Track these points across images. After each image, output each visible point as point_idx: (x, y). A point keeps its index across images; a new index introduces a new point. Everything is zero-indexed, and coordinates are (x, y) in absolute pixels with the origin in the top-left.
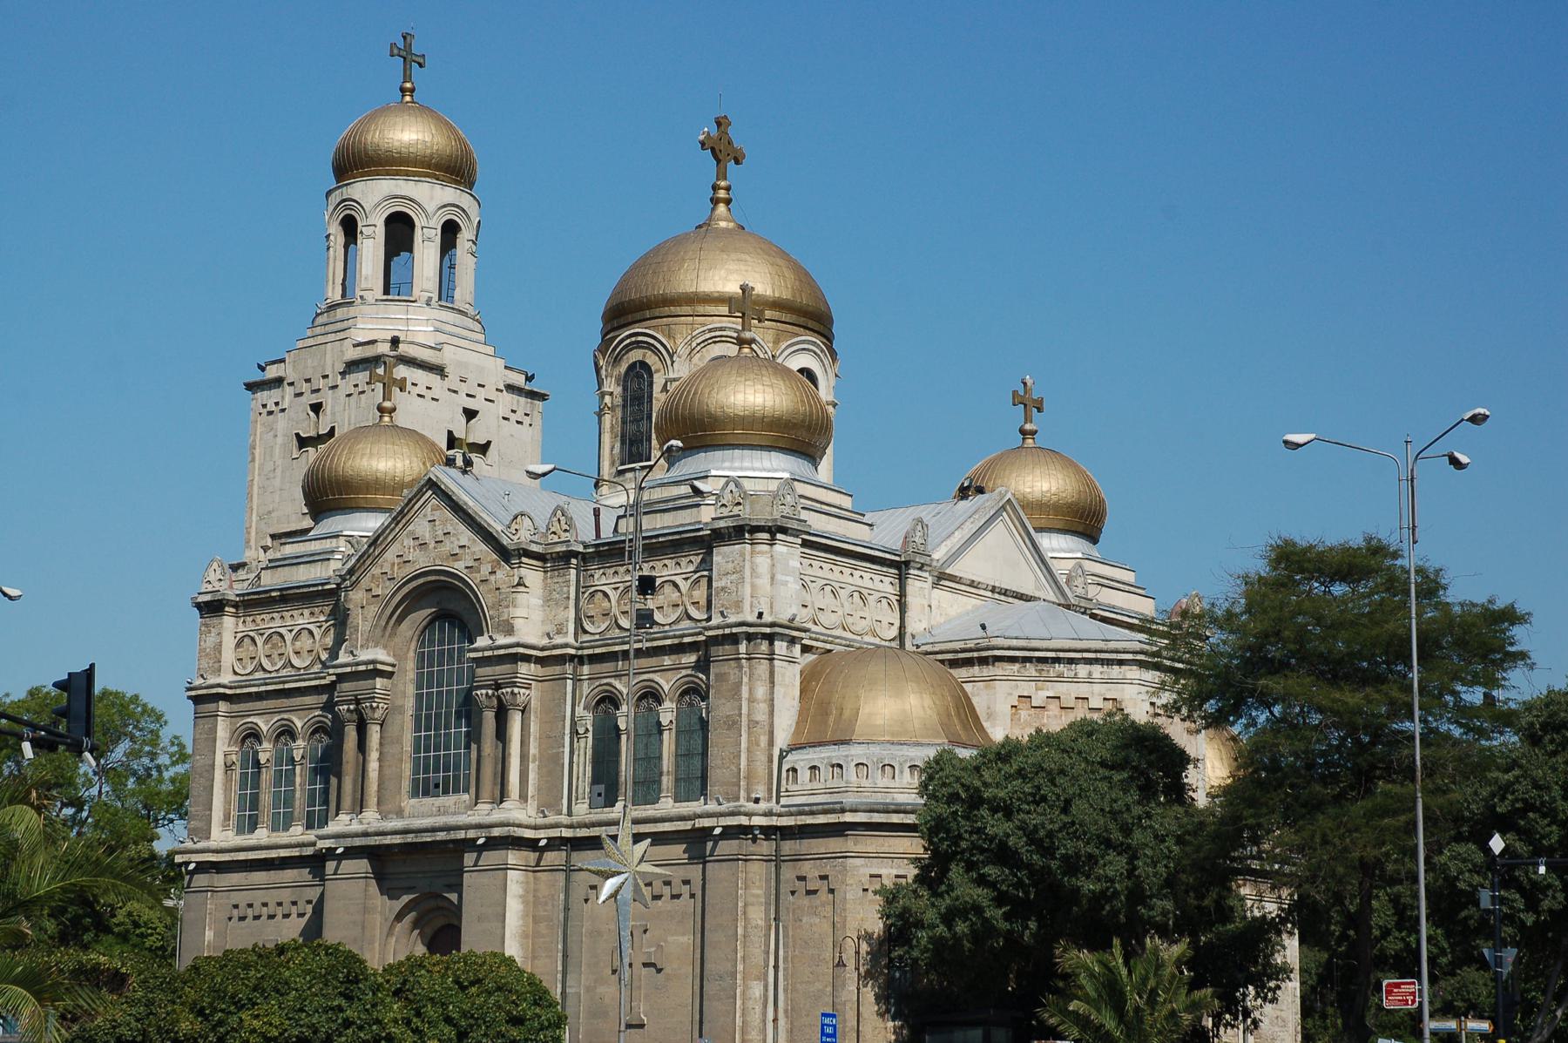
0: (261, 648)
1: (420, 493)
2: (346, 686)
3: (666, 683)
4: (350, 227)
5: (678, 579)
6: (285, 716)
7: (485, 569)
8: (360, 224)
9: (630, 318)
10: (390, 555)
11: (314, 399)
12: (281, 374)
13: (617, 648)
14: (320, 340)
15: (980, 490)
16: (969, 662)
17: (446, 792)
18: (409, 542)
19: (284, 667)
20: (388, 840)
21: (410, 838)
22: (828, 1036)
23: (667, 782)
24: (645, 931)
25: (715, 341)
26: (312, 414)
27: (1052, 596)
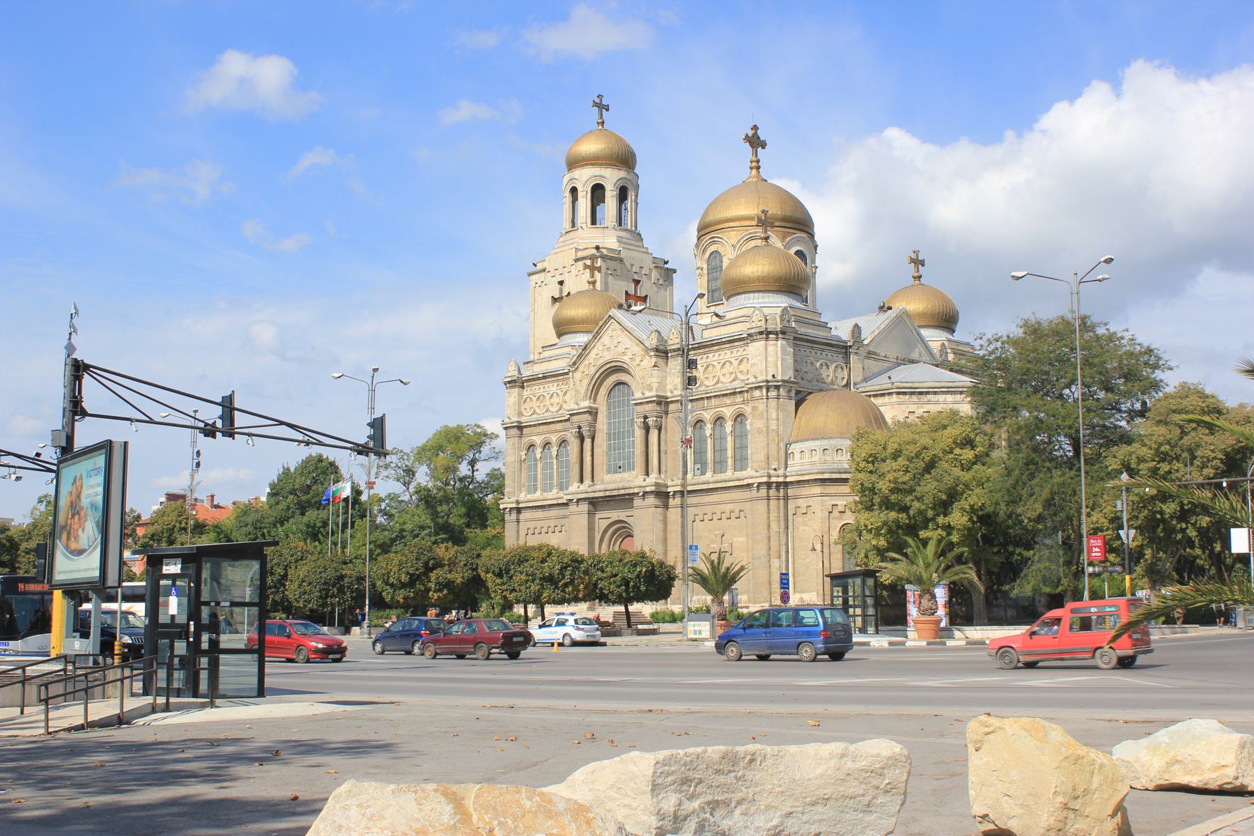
0: (535, 404)
1: (606, 323)
2: (575, 418)
3: (728, 412)
4: (574, 191)
5: (732, 360)
6: (547, 435)
7: (638, 359)
8: (579, 191)
9: (710, 229)
10: (592, 355)
12: (544, 266)
13: (704, 396)
14: (562, 249)
15: (890, 308)
16: (883, 395)
17: (624, 471)
18: (601, 347)
19: (547, 411)
20: (597, 495)
21: (608, 493)
22: (785, 584)
23: (730, 462)
24: (723, 536)
25: (751, 239)
26: (559, 286)
27: (927, 358)
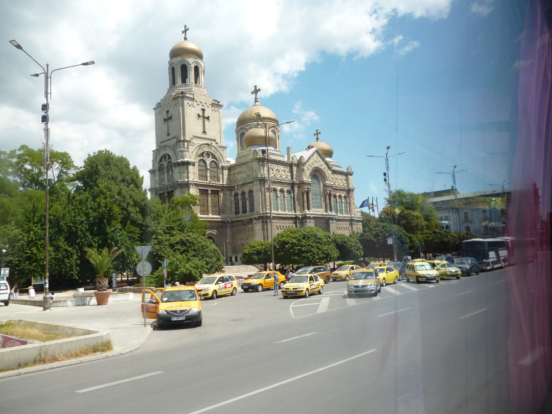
3: (343, 195)
10: (311, 161)
11: (203, 108)
18: (313, 160)
20: (319, 216)
21: (323, 216)
